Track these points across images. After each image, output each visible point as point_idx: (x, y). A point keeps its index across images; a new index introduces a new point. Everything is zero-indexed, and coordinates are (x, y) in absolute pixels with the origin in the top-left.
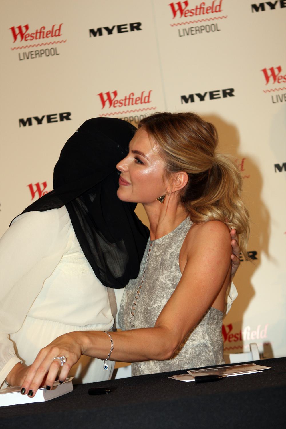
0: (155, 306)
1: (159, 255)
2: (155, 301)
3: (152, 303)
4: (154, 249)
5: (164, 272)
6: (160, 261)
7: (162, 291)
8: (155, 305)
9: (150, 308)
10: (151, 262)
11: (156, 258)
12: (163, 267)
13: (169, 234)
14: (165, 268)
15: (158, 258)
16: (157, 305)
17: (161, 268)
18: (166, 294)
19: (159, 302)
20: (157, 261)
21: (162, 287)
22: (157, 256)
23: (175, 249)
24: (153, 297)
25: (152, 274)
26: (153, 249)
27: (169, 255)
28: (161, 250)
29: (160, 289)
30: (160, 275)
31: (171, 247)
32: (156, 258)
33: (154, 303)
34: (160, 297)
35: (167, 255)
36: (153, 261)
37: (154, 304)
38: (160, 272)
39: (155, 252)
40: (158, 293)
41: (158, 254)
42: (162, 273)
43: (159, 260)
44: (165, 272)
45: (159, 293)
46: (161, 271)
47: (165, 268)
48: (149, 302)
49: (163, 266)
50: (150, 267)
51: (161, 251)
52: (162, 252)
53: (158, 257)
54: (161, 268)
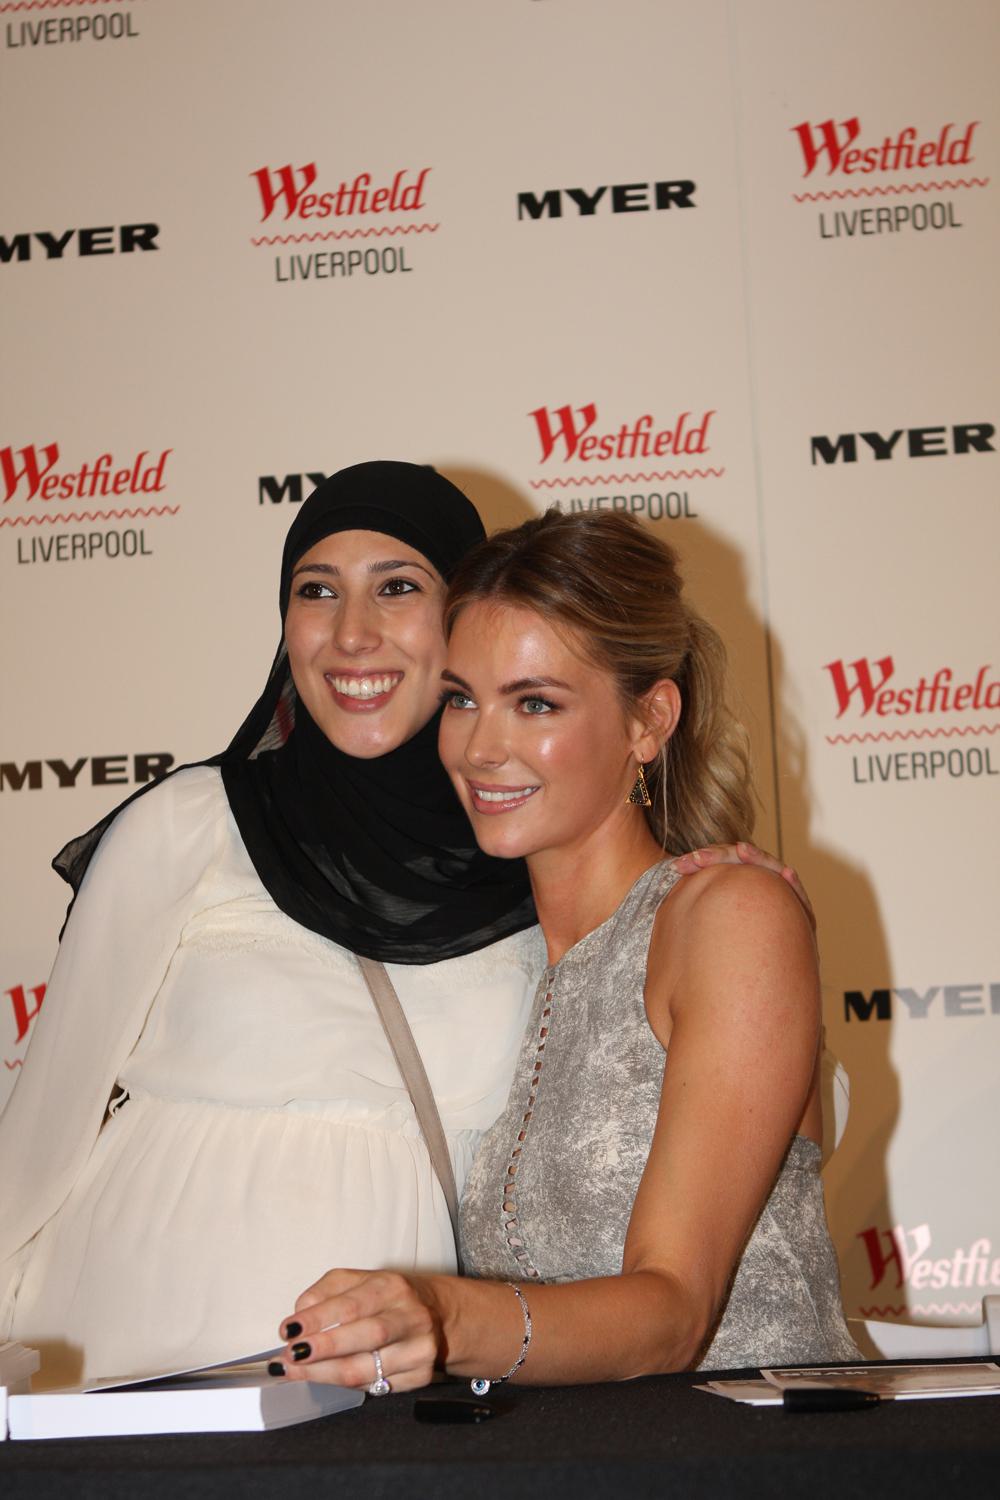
0: (579, 1146)
2: (577, 1132)
3: (568, 1140)
7: (602, 1096)
8: (579, 1142)
9: (565, 1155)
16: (585, 1142)
18: (616, 1103)
19: (593, 1132)
21: (601, 1082)
24: (571, 1124)
29: (591, 1091)
33: (577, 1138)
34: (595, 1118)
37: (576, 1142)
40: (587, 1107)
45: (591, 1104)
48: (558, 1140)
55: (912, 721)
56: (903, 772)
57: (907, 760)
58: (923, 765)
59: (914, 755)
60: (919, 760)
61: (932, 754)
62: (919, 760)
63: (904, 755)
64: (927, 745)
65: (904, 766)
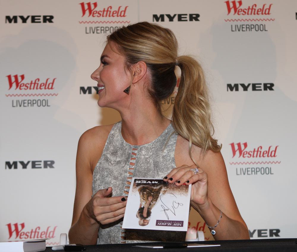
1: (149, 157)
5: (159, 173)
6: (152, 162)
10: (141, 165)
11: (146, 160)
12: (158, 168)
13: (157, 138)
14: (159, 169)
15: (148, 160)
17: (155, 169)
20: (148, 163)
23: (168, 153)
25: (145, 175)
30: (156, 176)
35: (159, 157)
36: (143, 164)
38: (155, 173)
39: (144, 155)
42: (158, 174)
43: (150, 162)
44: (161, 173)
46: (156, 172)
47: (159, 169)
49: (157, 167)
50: (142, 169)
53: (149, 159)
54: (156, 170)
55: (252, 159)
56: (249, 173)
57: (250, 170)
58: (254, 171)
59: (252, 168)
60: (253, 170)
61: (257, 168)
62: (253, 170)
63: (249, 168)
64: (255, 166)
65: (249, 171)
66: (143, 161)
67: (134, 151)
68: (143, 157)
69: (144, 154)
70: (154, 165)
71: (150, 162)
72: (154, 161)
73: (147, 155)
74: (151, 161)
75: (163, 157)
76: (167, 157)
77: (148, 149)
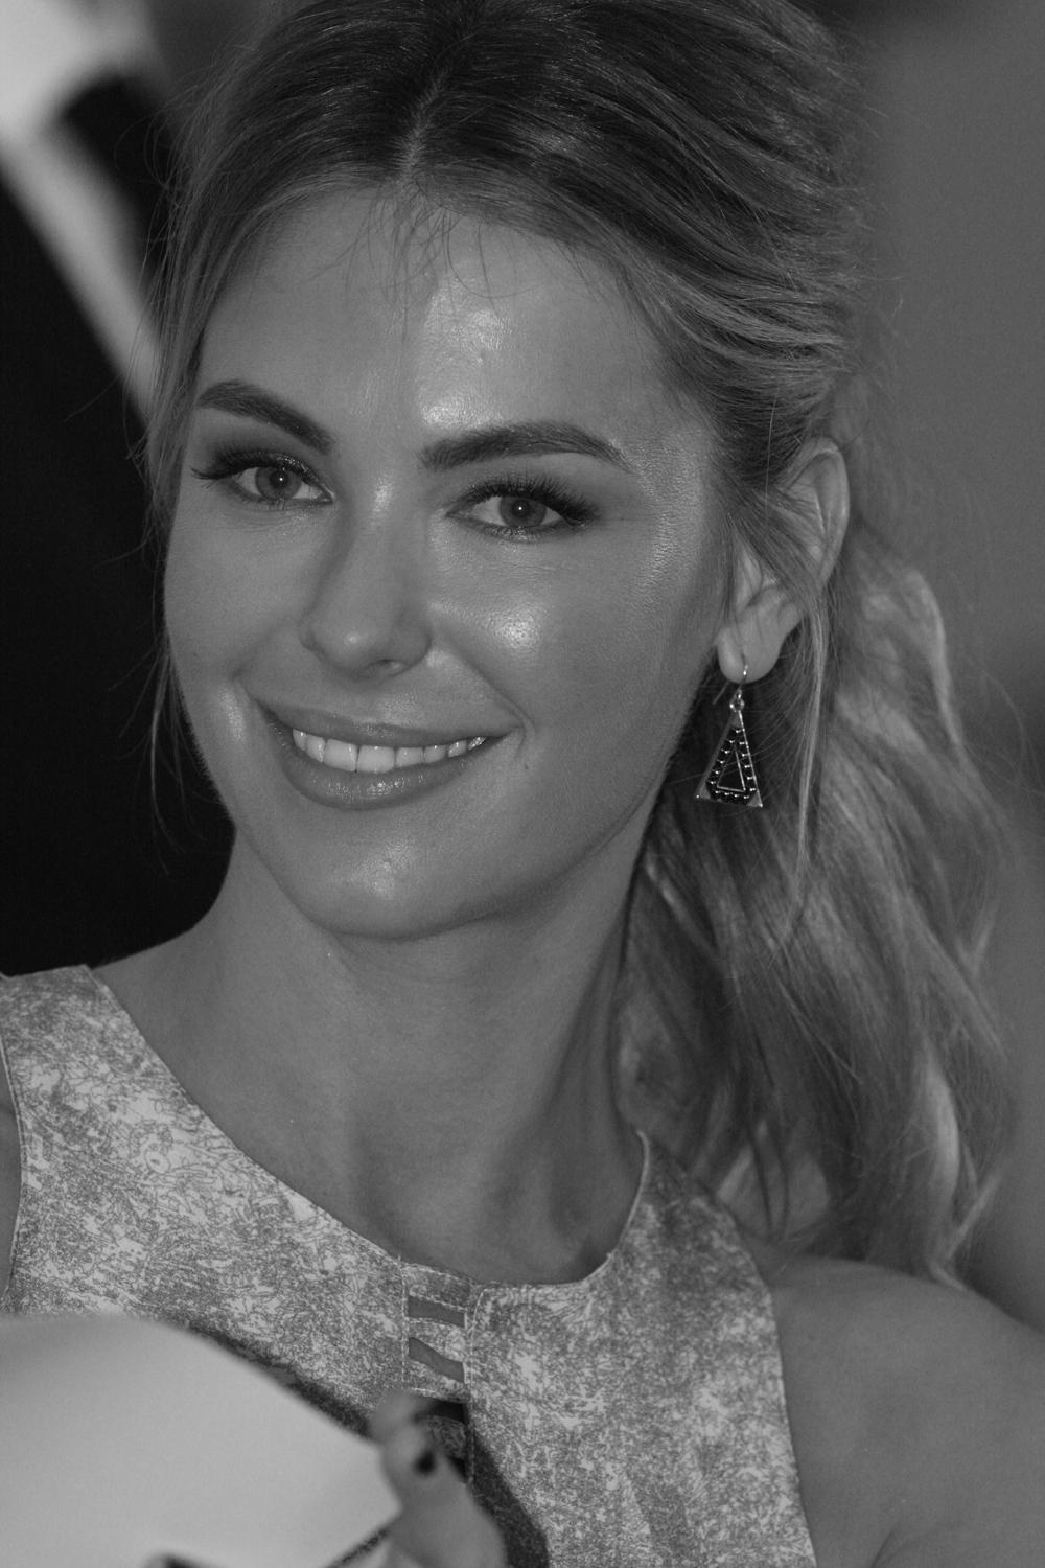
1: (588, 1435)
4: (515, 1369)
6: (630, 1492)
11: (567, 1459)
22: (569, 1441)
26: (504, 1369)
27: (688, 1458)
28: (592, 1388)
31: (682, 1389)
32: (567, 1459)
36: (547, 1486)
41: (570, 1422)
43: (611, 1485)
51: (598, 1403)
52: (614, 1410)
66: (541, 1460)
67: (434, 1330)
68: (531, 1416)
69: (533, 1385)
70: (649, 1517)
71: (611, 1485)
72: (635, 1479)
73: (568, 1407)
74: (615, 1477)
75: (709, 1456)
76: (736, 1466)
77: (564, 1351)
